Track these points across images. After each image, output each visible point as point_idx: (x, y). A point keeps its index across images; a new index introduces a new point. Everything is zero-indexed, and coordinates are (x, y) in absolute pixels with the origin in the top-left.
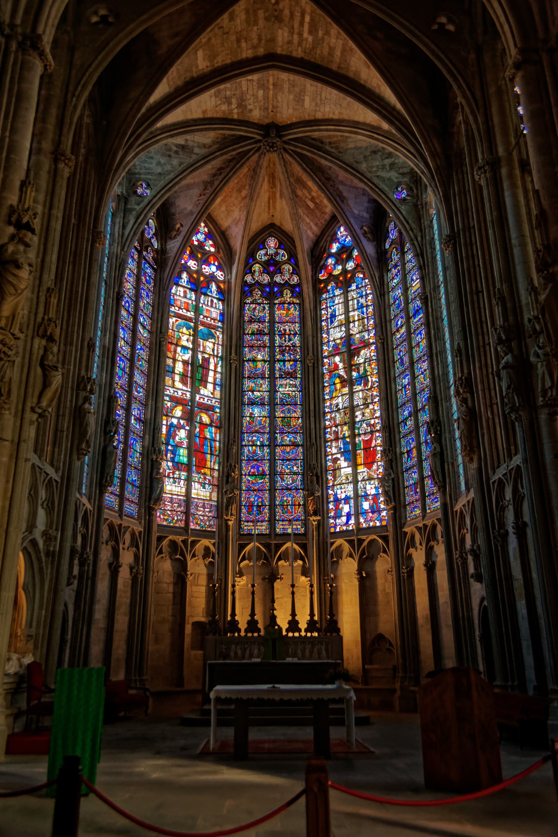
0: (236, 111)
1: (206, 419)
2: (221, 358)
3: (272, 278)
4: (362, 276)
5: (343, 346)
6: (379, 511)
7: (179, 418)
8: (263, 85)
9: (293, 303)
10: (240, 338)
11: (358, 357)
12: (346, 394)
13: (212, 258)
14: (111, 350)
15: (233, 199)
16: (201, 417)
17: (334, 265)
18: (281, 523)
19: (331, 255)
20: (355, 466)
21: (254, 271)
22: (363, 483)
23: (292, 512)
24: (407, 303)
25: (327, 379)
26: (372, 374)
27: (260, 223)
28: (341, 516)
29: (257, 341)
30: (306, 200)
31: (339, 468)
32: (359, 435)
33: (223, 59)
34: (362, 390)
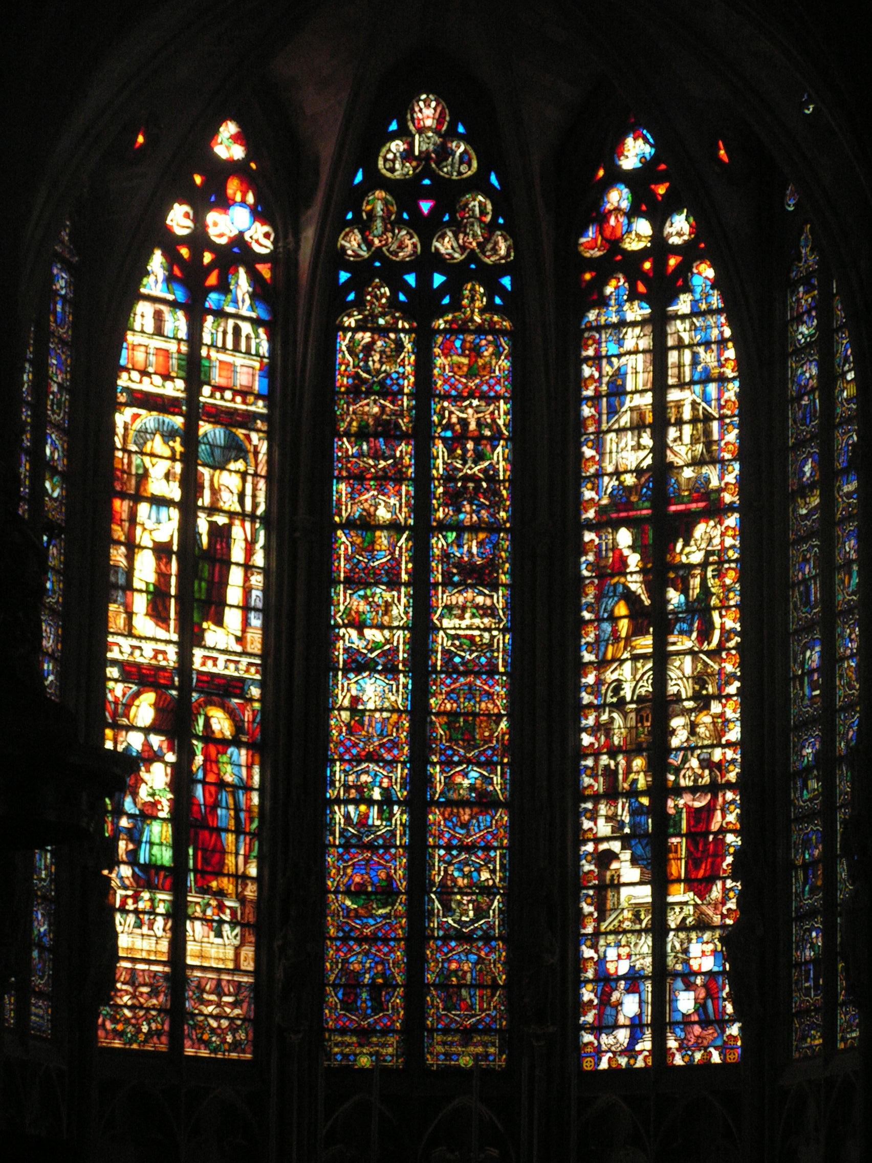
1: (221, 723)
2: (266, 520)
3: (426, 243)
5: (641, 496)
6: (722, 1023)
7: (146, 731)
10: (325, 455)
11: (686, 544)
12: (644, 657)
16: (207, 720)
18: (438, 1038)
19: (617, 176)
21: (371, 215)
22: (682, 935)
23: (471, 1007)
25: (590, 599)
26: (724, 607)
28: (616, 1026)
29: (377, 455)
31: (617, 886)
32: (678, 791)
34: (691, 652)
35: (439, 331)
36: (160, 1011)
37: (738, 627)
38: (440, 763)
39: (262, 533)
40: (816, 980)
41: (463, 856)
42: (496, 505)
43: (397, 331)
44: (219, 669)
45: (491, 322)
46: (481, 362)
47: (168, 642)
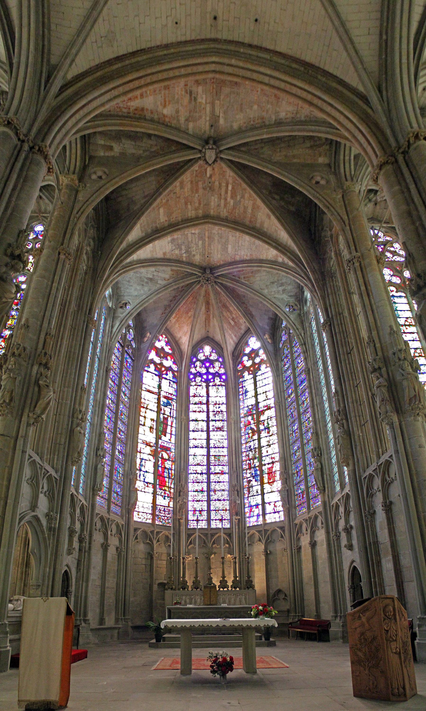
0: (184, 255)
8: (202, 237)
14: (101, 403)
15: (183, 319)
24: (295, 378)
27: (200, 336)
33: (177, 216)
39: (175, 421)
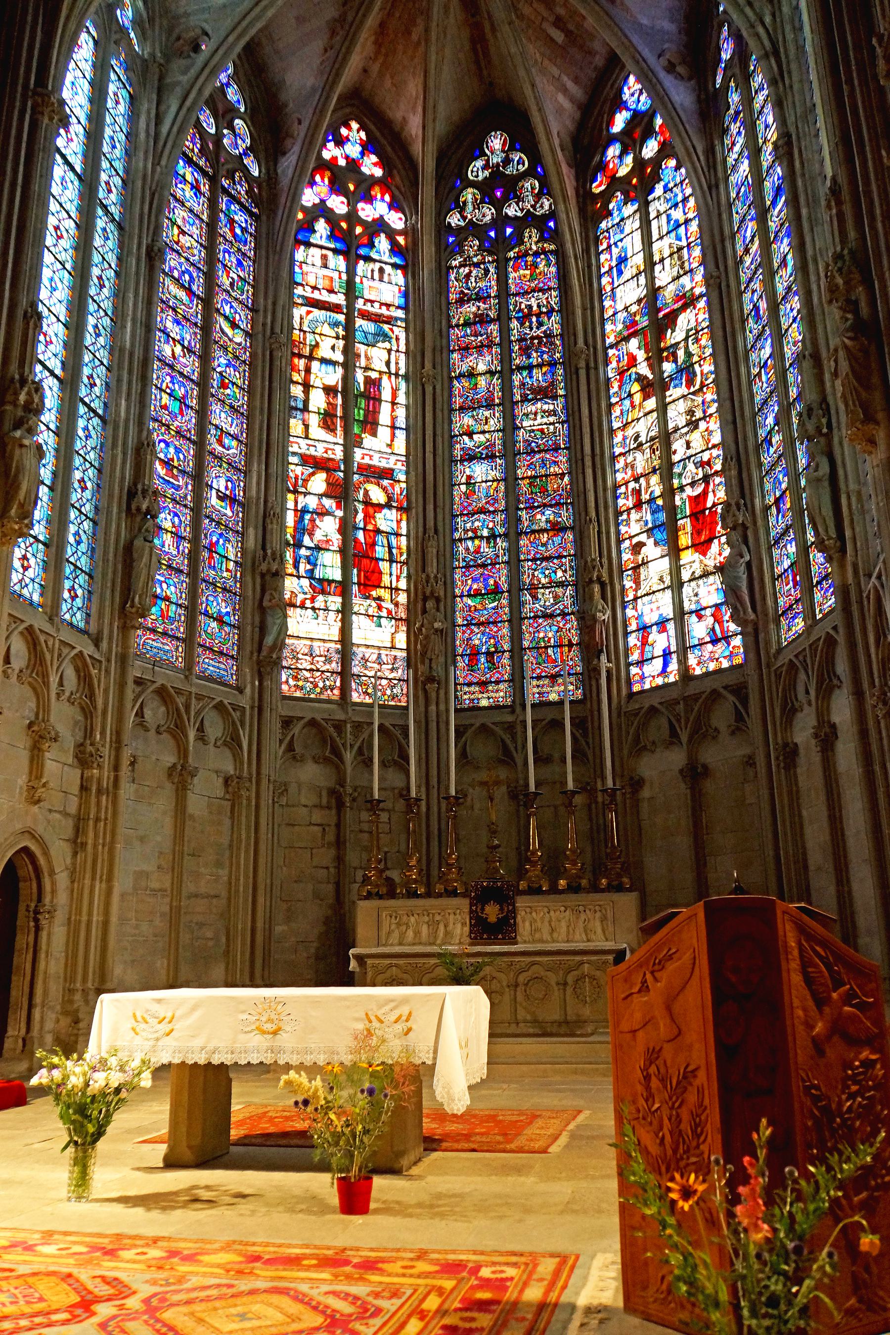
1: (377, 495)
2: (406, 377)
3: (499, 210)
4: (672, 163)
6: (727, 638)
7: (321, 496)
9: (544, 252)
11: (673, 331)
13: (377, 189)
16: (366, 492)
17: (620, 157)
18: (535, 682)
19: (613, 139)
20: (675, 552)
21: (465, 203)
22: (693, 584)
28: (653, 658)
29: (476, 335)
30: (545, 25)
32: (682, 488)
34: (684, 396)
35: (510, 259)
36: (333, 673)
37: (712, 368)
38: (526, 508)
40: (794, 580)
41: (544, 564)
42: (552, 352)
43: (484, 263)
44: (375, 462)
45: (543, 249)
46: (538, 271)
47: (335, 444)
